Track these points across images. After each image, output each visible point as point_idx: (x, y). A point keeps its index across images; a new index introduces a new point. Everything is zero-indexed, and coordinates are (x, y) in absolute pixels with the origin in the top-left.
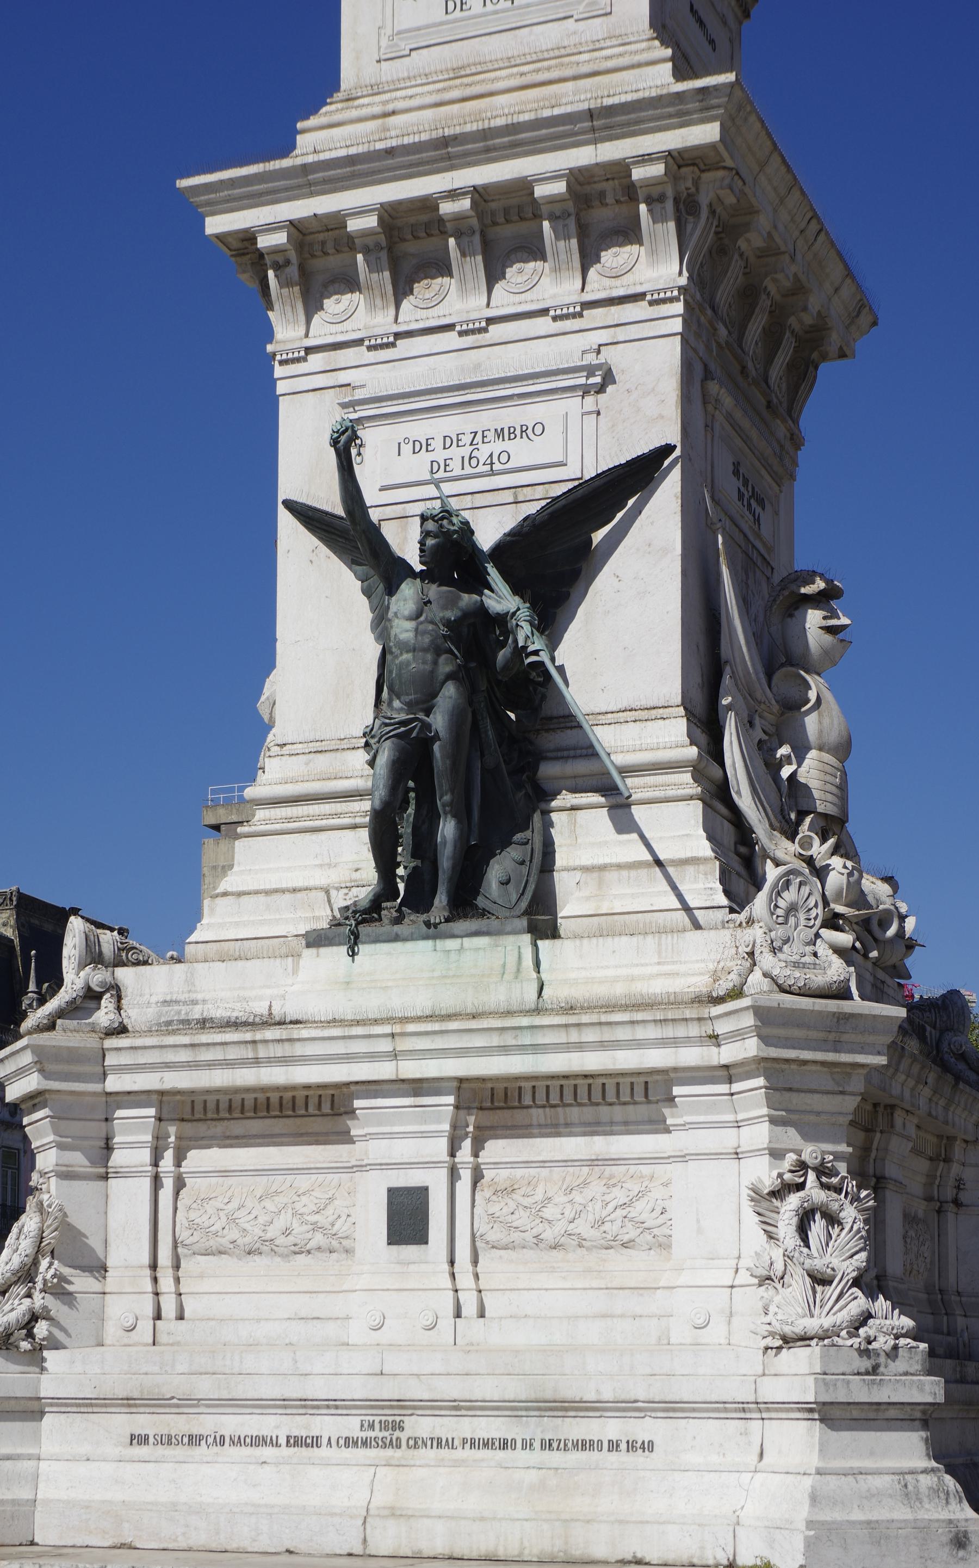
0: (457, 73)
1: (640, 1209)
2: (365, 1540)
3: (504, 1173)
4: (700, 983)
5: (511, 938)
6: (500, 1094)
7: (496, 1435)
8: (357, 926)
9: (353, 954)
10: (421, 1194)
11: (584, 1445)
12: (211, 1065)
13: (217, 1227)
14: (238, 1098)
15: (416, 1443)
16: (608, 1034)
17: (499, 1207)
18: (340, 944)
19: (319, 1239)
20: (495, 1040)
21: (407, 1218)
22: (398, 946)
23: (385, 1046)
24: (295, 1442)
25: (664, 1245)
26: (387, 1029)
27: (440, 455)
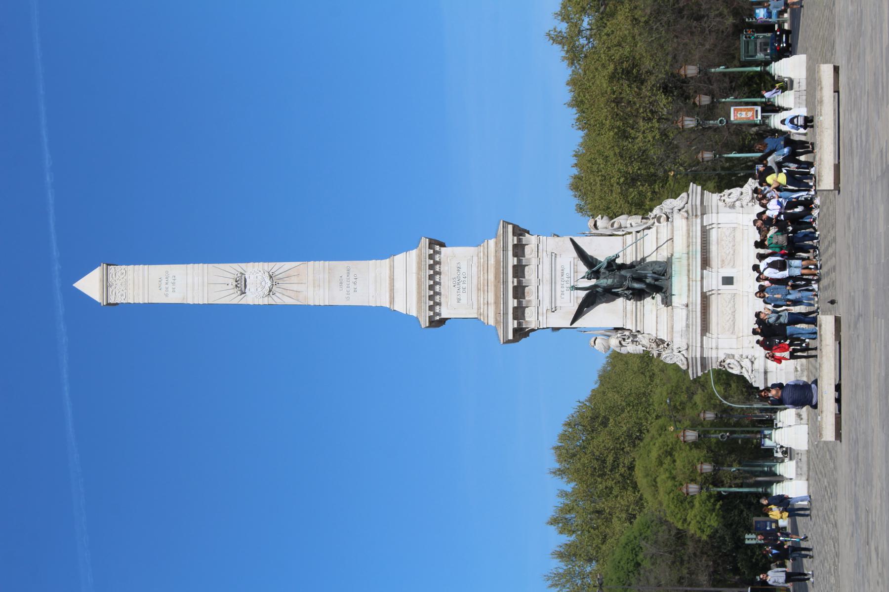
0: (479, 290)
4: (684, 221)
8: (667, 302)
17: (726, 263)
21: (728, 281)
25: (734, 228)
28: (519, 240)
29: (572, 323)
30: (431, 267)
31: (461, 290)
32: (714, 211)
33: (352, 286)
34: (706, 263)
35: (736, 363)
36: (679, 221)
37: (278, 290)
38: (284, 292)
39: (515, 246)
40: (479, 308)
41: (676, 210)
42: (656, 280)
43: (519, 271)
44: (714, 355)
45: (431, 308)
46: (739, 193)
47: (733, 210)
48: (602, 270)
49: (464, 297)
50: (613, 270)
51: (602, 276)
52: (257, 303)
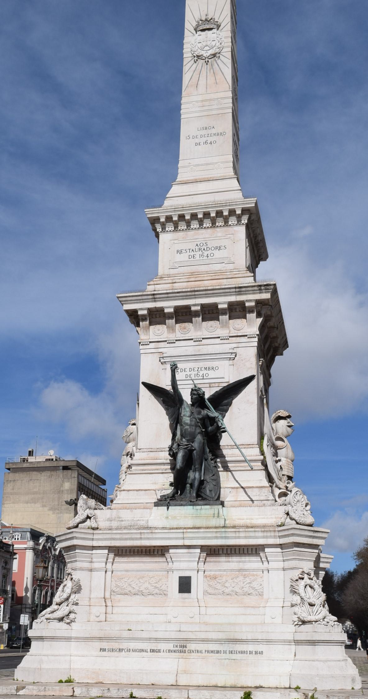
0: (192, 274)
1: (254, 584)
2: (177, 681)
3: (213, 573)
5: (216, 506)
6: (213, 550)
7: (215, 649)
8: (165, 501)
9: (168, 509)
10: (189, 578)
11: (242, 652)
12: (126, 539)
13: (125, 586)
14: (133, 549)
15: (191, 651)
16: (248, 534)
17: (212, 583)
18: (165, 506)
19: (157, 591)
20: (214, 535)
21: (185, 585)
22: (182, 507)
23: (181, 535)
24: (153, 651)
25: (261, 595)
26: (182, 531)
27: (188, 373)
28: (251, 311)
29: (144, 384)
30: (219, 214)
31: (192, 253)
32: (287, 564)
33: (204, 139)
34: (212, 551)
35: (65, 596)
36: (272, 515)
37: (200, 65)
38: (197, 72)
39: (242, 303)
40: (169, 276)
41: (289, 508)
42: (192, 485)
43: (210, 313)
44: (78, 565)
45: (169, 219)
46: (312, 601)
47: (288, 589)
48: (205, 412)
49: (184, 257)
50: (204, 426)
51: (195, 410)
52: (185, 46)
